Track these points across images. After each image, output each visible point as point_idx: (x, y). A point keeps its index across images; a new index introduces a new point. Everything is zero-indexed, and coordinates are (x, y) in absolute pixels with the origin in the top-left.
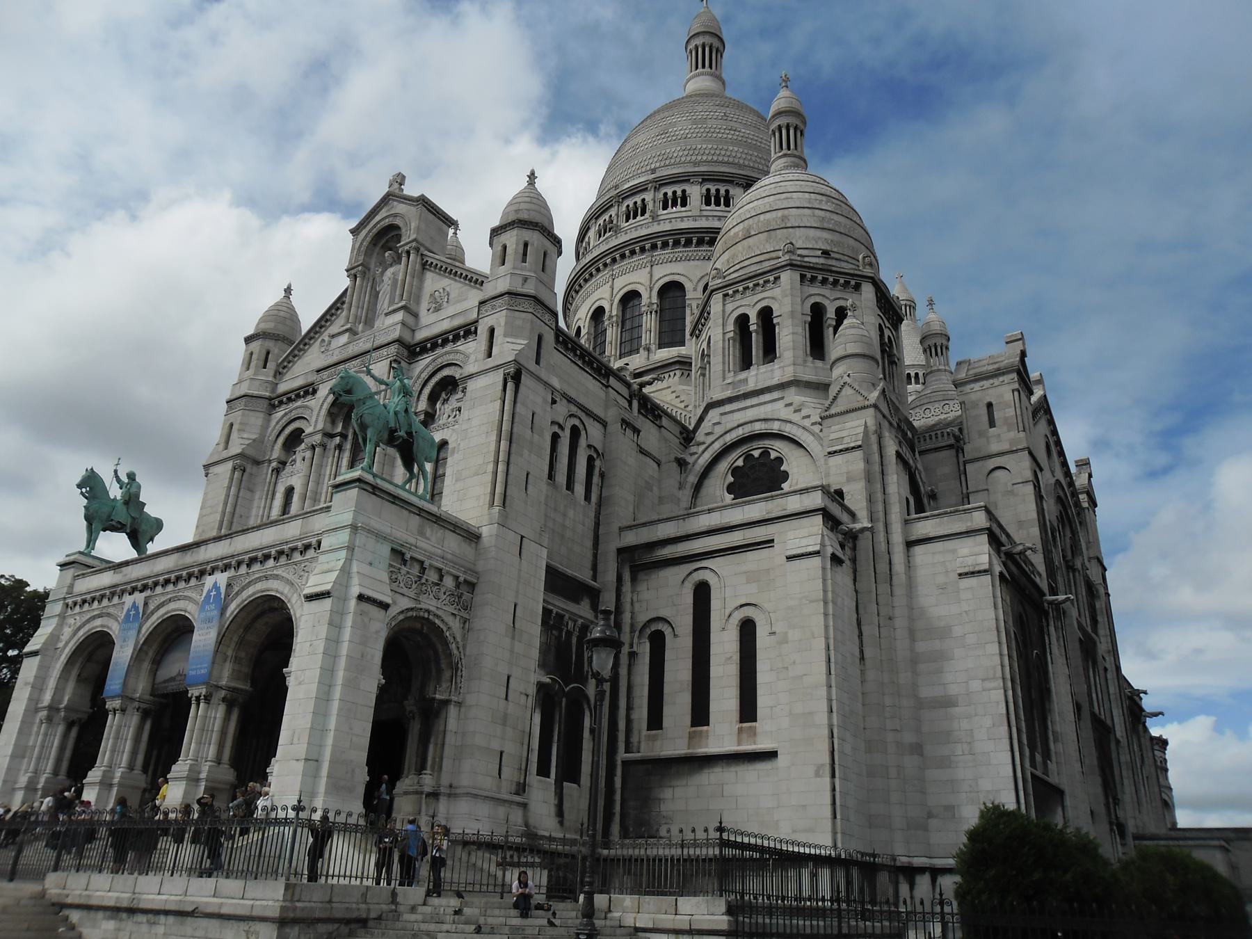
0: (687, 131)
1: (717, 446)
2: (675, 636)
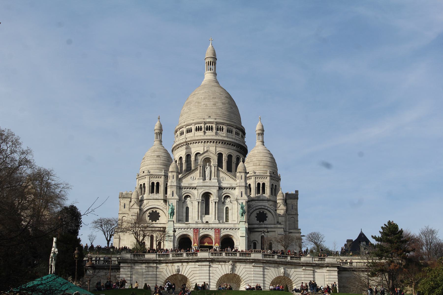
0: (221, 107)
1: (255, 209)
2: (258, 243)
